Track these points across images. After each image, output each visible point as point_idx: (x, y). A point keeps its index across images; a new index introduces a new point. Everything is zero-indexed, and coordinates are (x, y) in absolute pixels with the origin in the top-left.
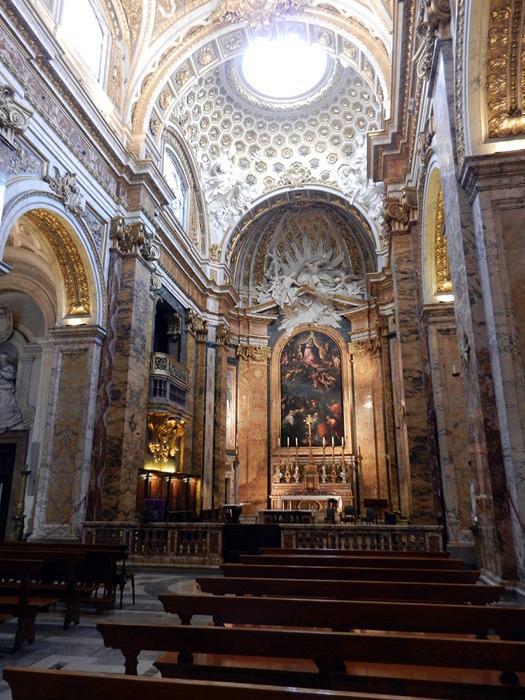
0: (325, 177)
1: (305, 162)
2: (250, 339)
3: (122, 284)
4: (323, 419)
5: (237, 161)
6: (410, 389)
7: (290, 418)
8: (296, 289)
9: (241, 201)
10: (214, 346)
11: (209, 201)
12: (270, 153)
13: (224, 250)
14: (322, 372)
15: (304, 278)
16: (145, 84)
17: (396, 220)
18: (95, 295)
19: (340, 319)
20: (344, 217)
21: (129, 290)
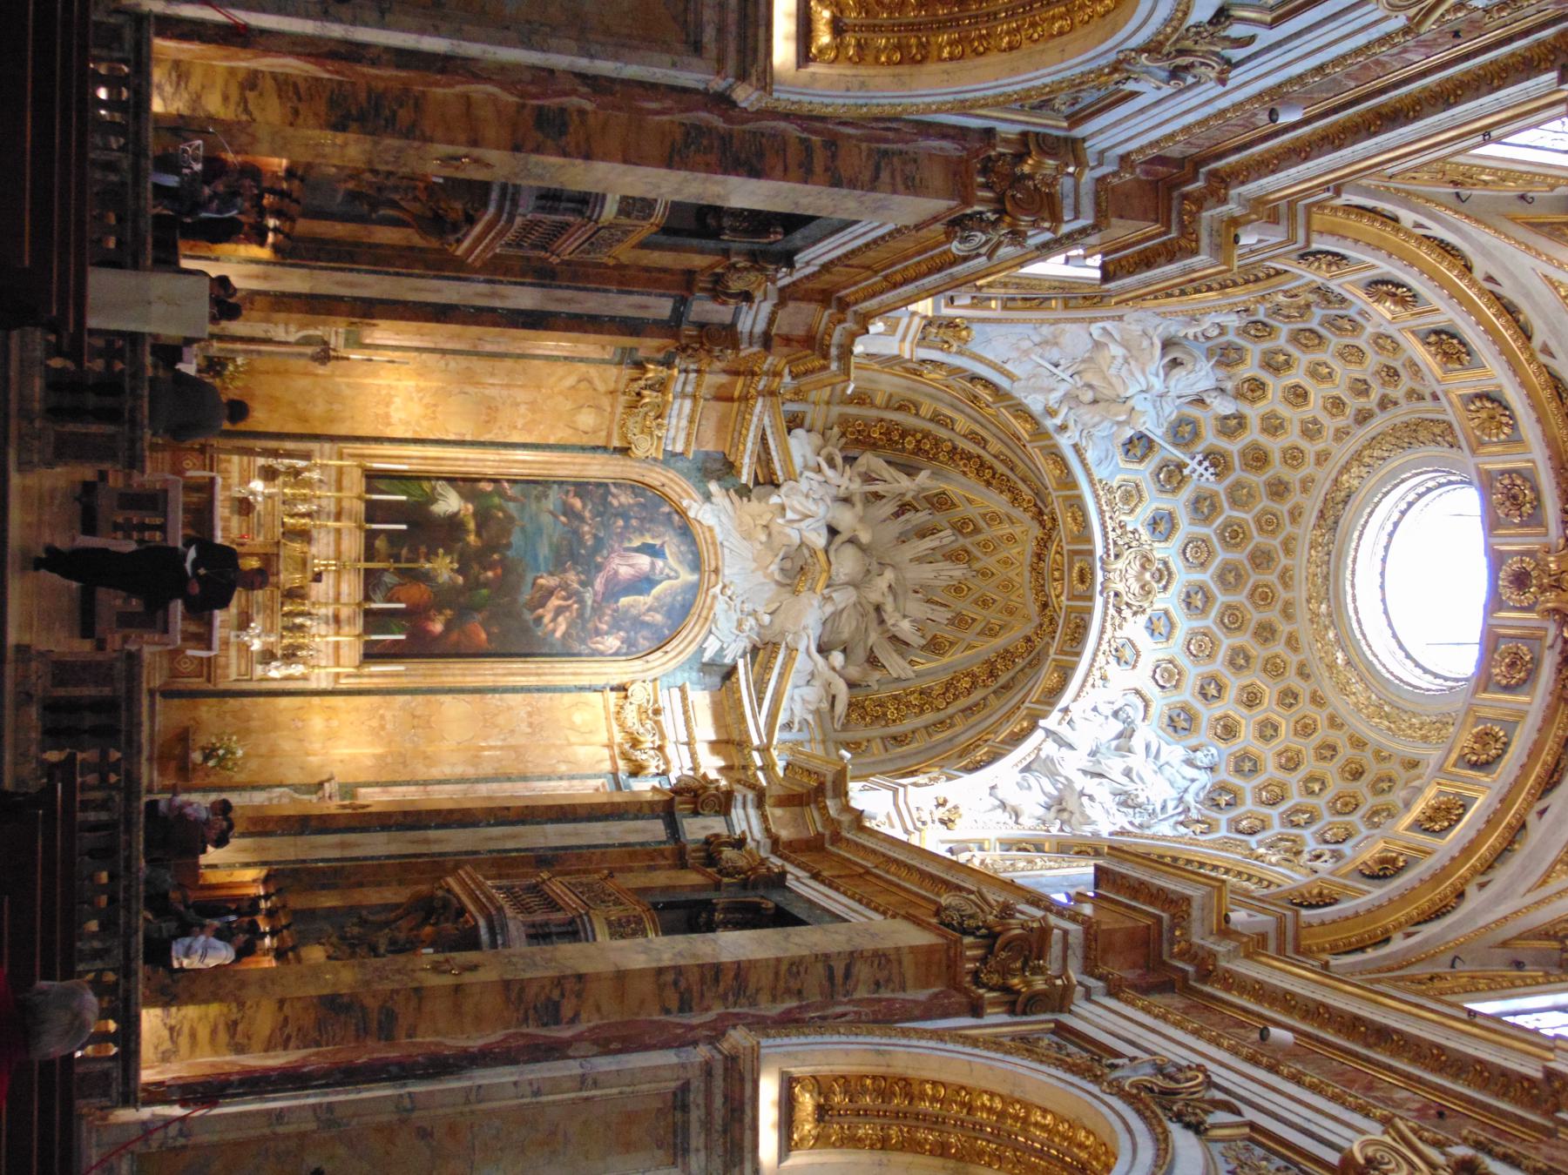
2: (688, 404)
3: (885, 153)
4: (443, 599)
5: (1195, 412)
6: (532, 991)
7: (450, 503)
8: (819, 540)
9: (1088, 415)
10: (678, 316)
11: (1095, 329)
14: (581, 601)
15: (847, 563)
16: (1445, 248)
17: (990, 950)
18: (863, 86)
19: (728, 660)
20: (1006, 687)
21: (866, 176)
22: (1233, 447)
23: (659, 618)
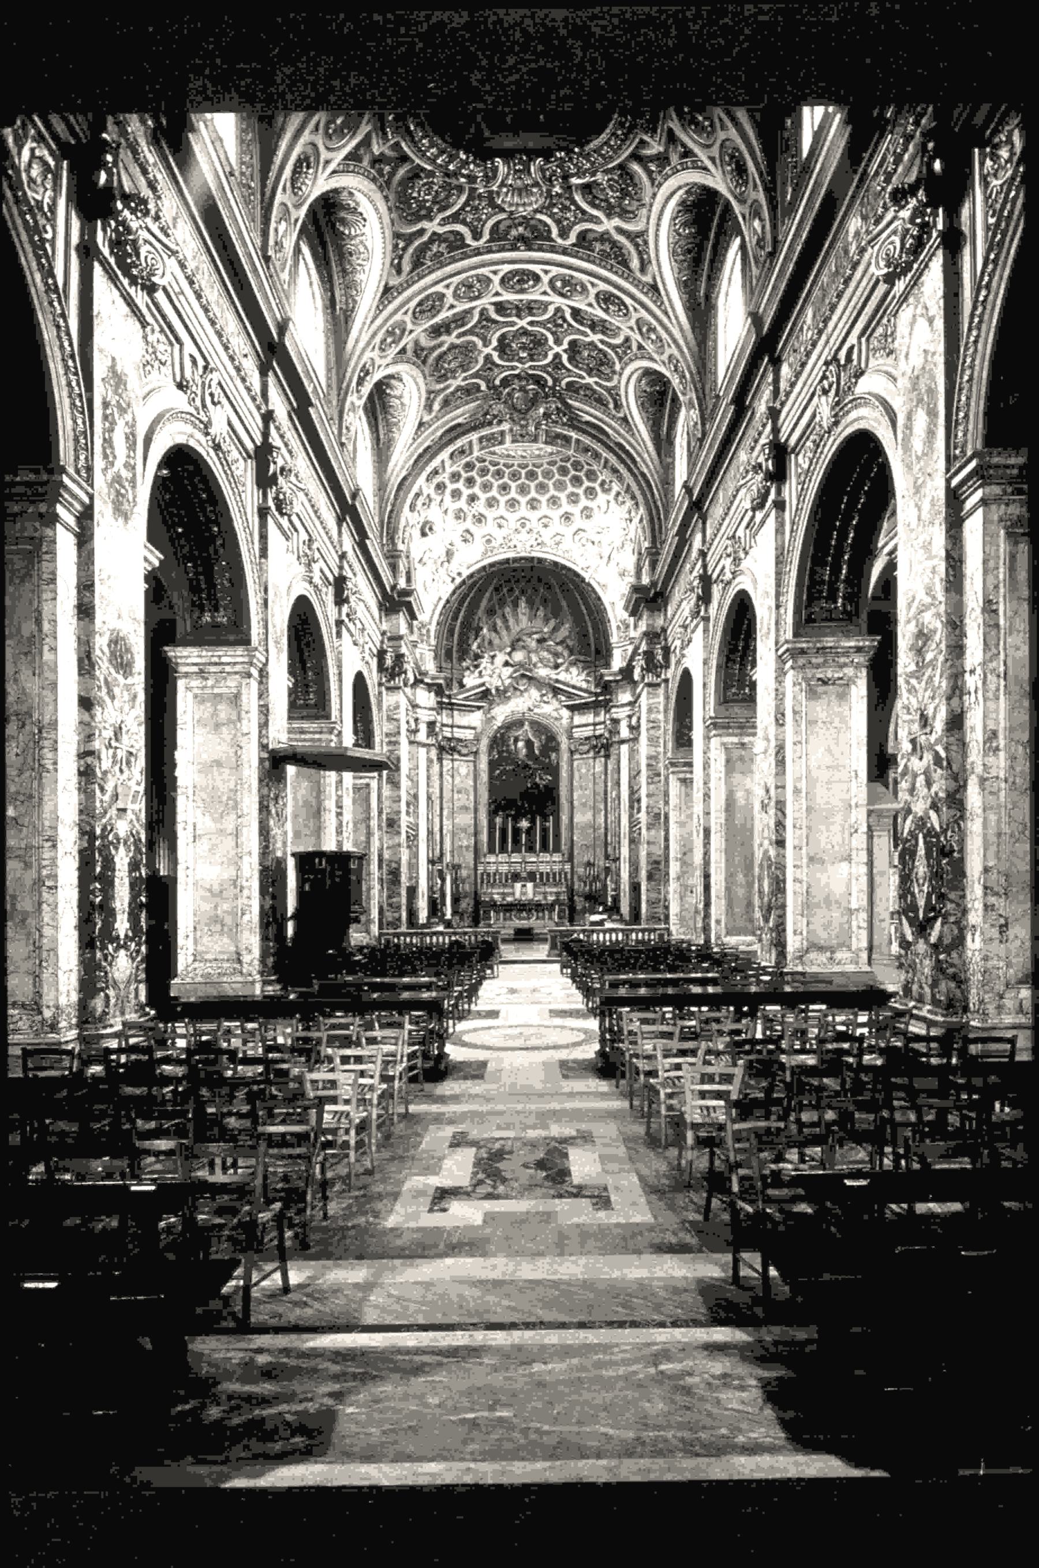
8: (511, 669)
10: (424, 745)
13: (433, 628)
15: (519, 656)
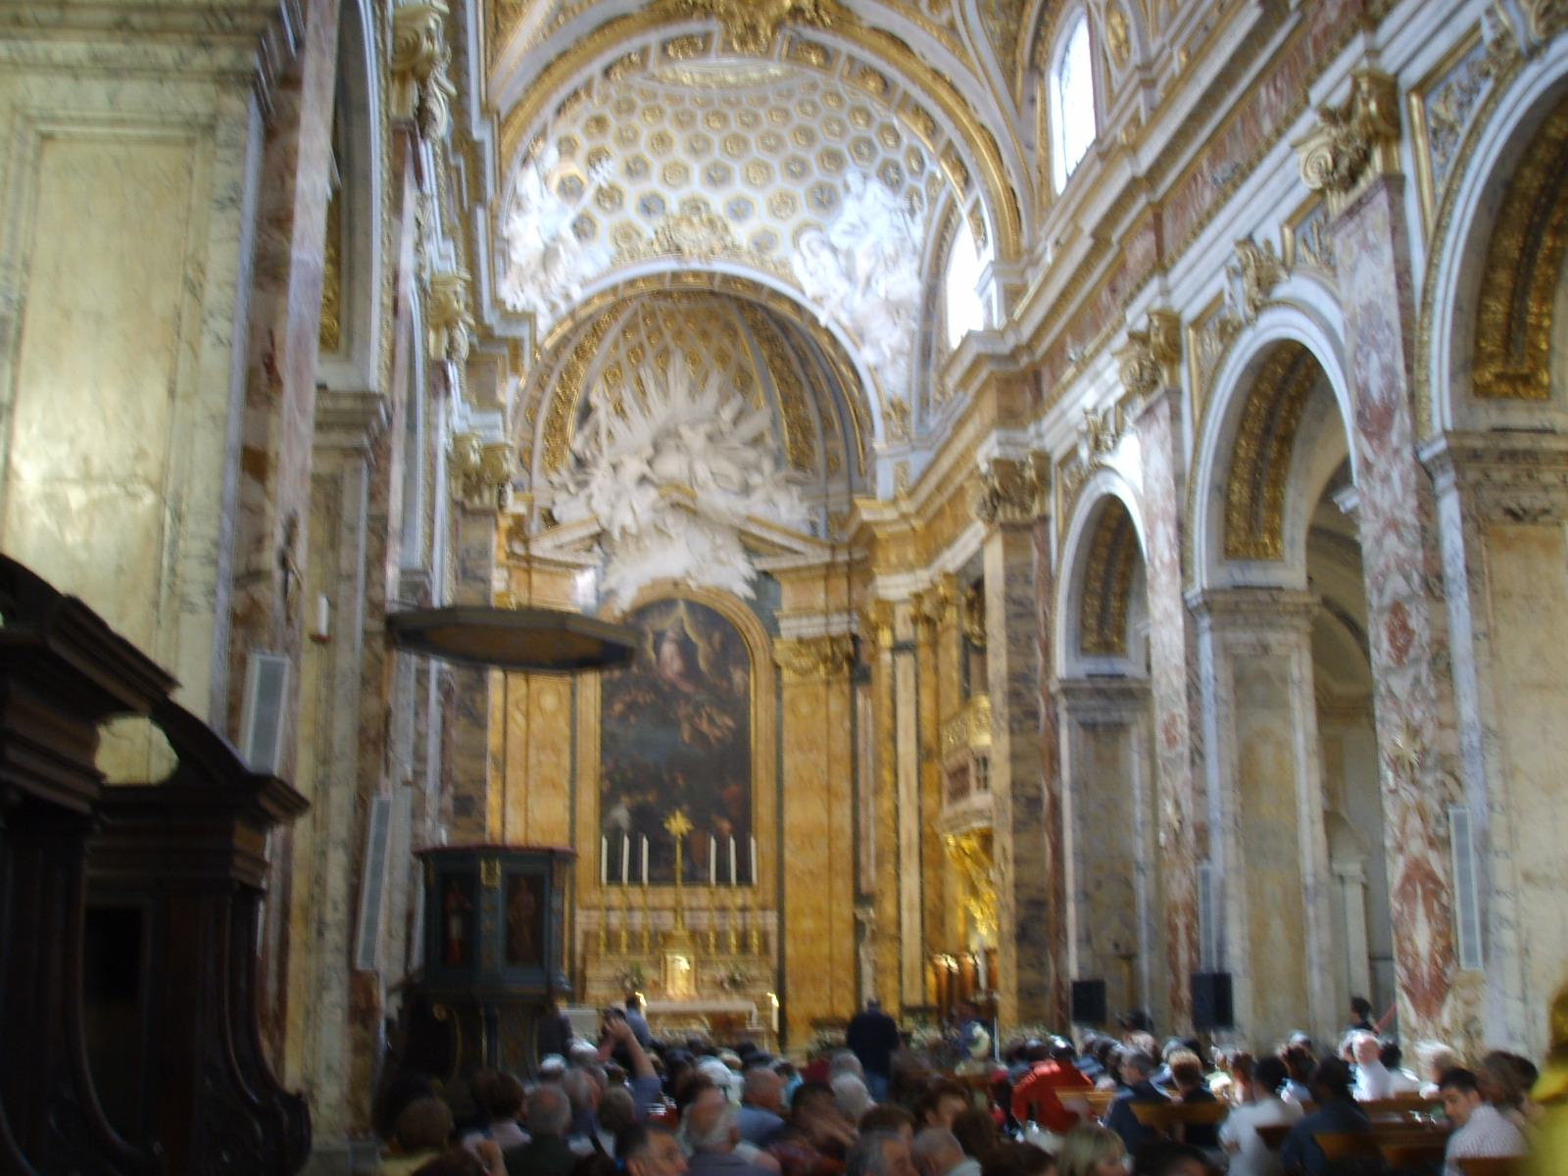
0: (763, 243)
1: (718, 202)
5: (555, 182)
7: (621, 814)
9: (560, 275)
12: (635, 169)
15: (671, 466)
17: (1010, 500)
19: (754, 576)
21: (481, 586)
22: (585, 145)
23: (717, 637)
